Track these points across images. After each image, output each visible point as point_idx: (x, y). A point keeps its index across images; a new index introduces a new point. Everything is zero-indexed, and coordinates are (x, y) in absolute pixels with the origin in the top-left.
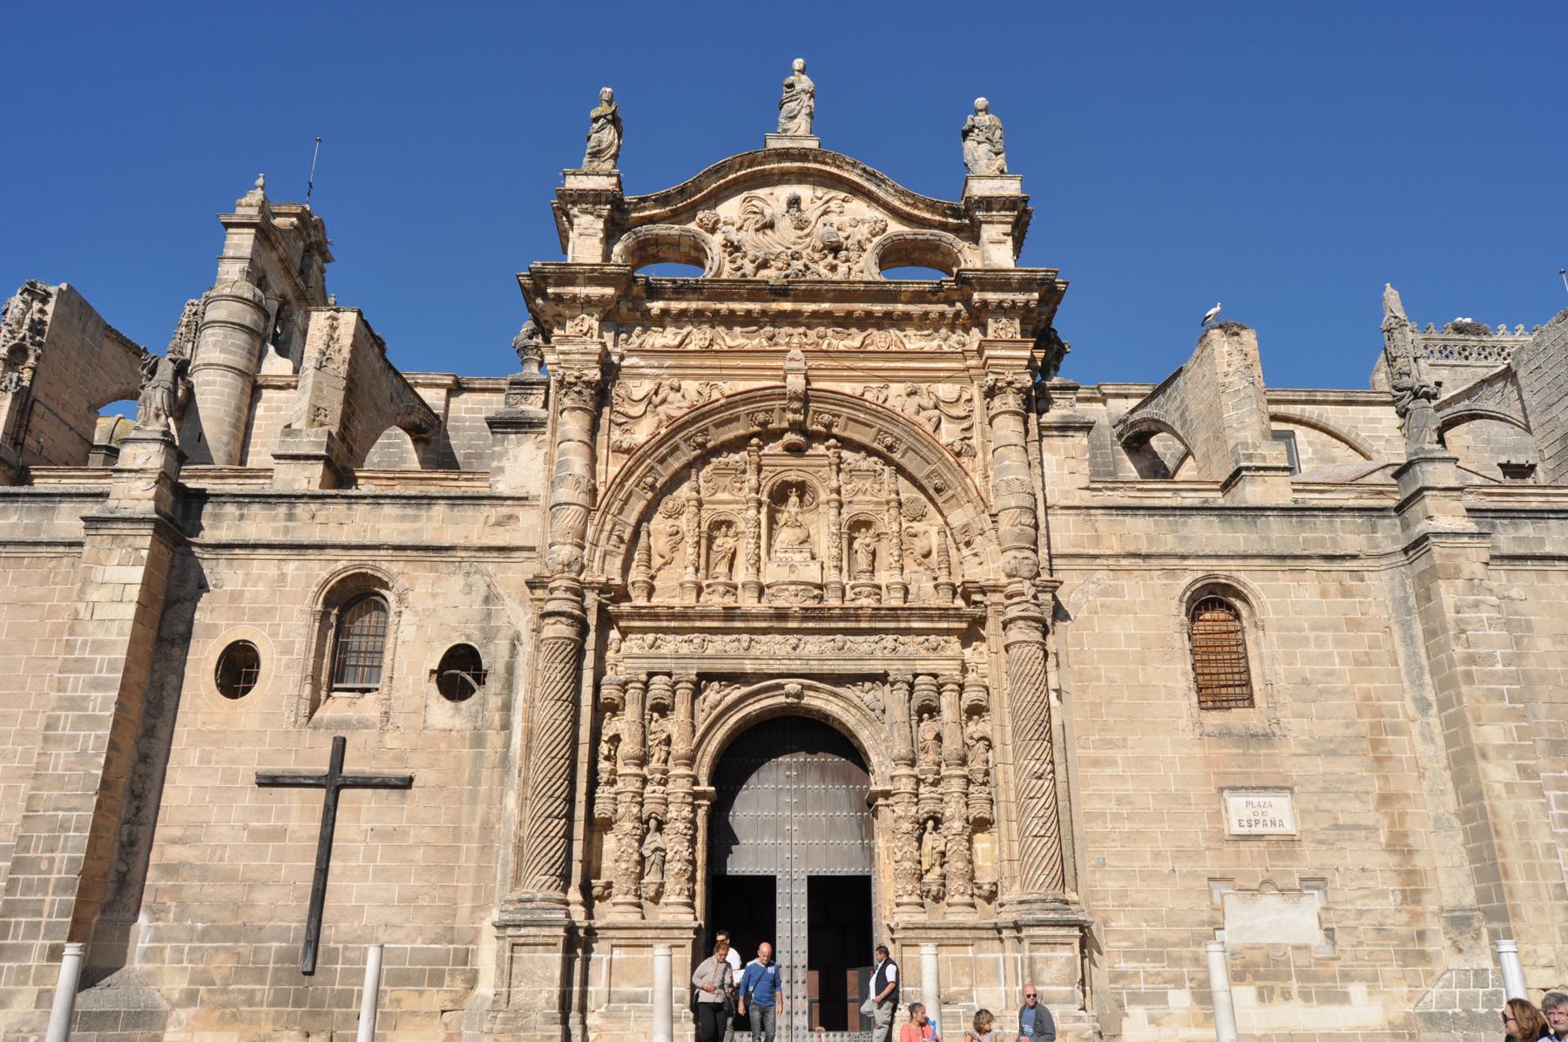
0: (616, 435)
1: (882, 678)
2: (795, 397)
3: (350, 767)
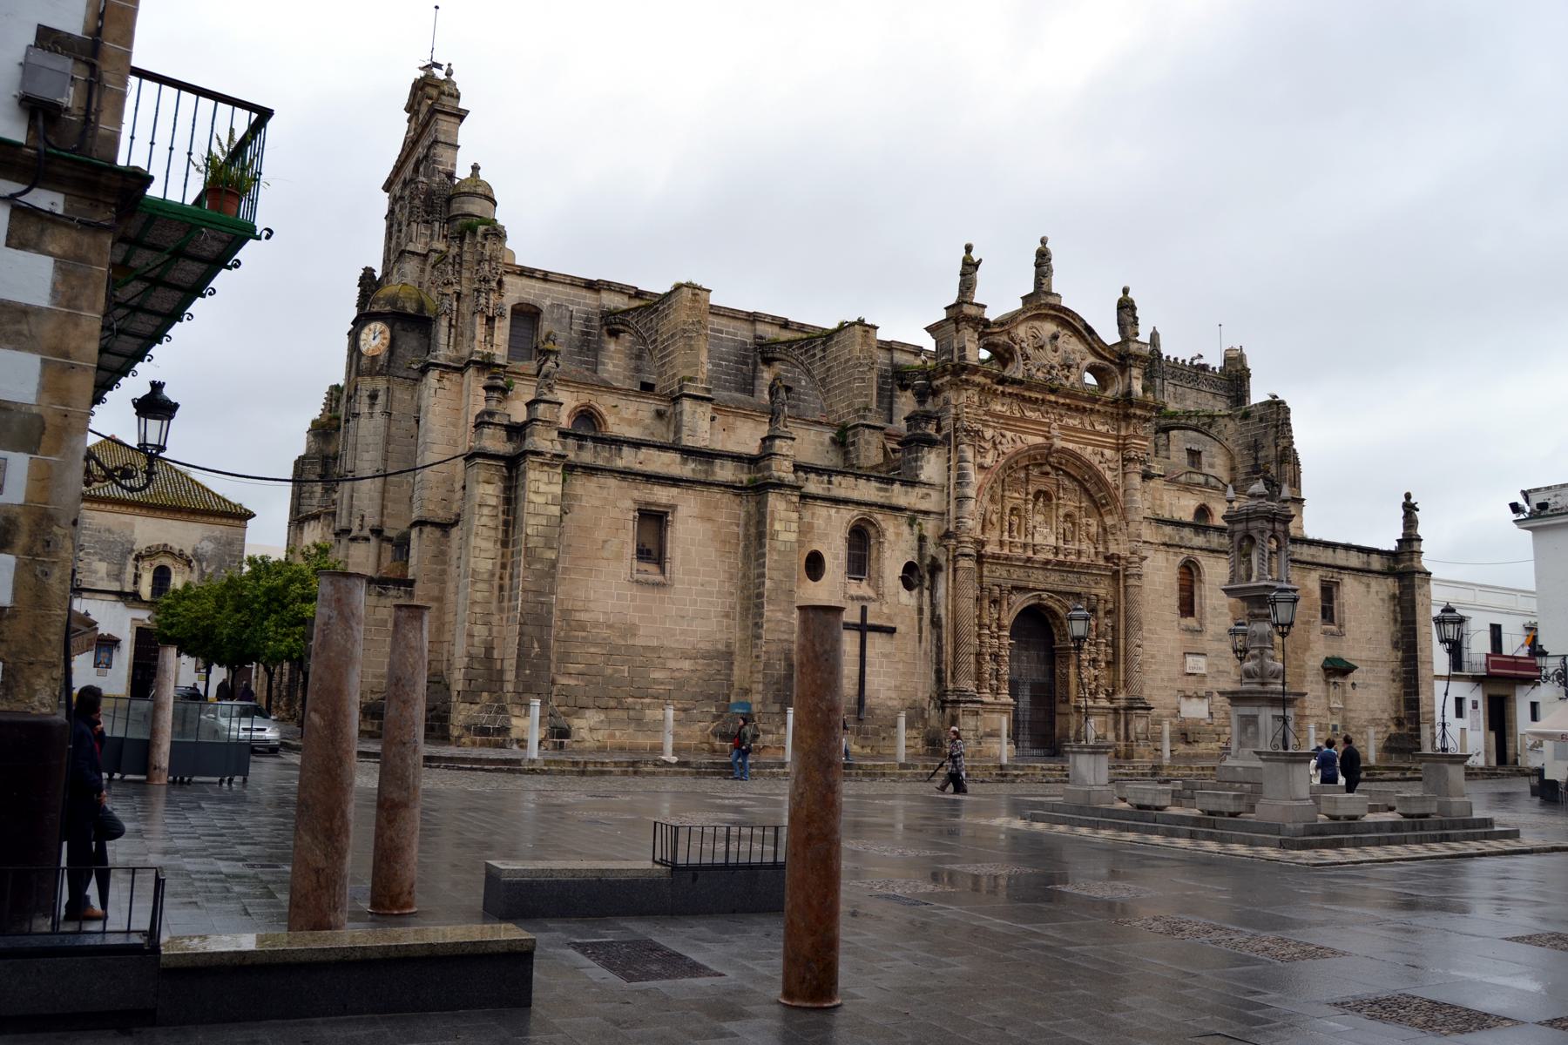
0: (979, 460)
1: (1078, 596)
2: (1057, 451)
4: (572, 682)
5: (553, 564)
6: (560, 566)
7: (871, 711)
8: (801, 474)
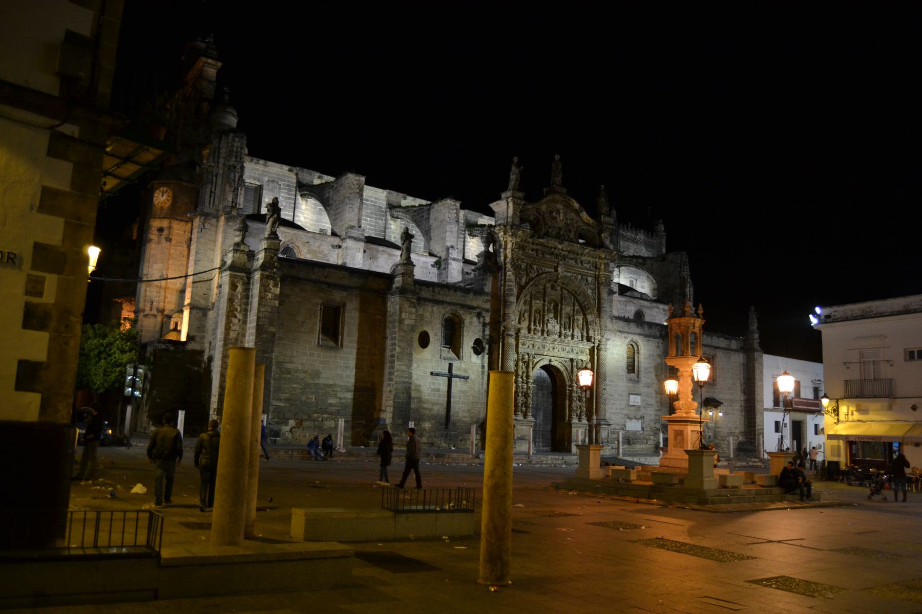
3: (454, 372)
4: (282, 404)
5: (274, 334)
6: (277, 336)
7: (454, 424)
8: (417, 286)
